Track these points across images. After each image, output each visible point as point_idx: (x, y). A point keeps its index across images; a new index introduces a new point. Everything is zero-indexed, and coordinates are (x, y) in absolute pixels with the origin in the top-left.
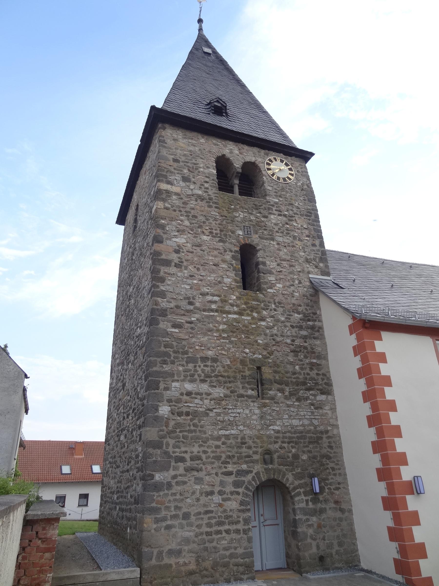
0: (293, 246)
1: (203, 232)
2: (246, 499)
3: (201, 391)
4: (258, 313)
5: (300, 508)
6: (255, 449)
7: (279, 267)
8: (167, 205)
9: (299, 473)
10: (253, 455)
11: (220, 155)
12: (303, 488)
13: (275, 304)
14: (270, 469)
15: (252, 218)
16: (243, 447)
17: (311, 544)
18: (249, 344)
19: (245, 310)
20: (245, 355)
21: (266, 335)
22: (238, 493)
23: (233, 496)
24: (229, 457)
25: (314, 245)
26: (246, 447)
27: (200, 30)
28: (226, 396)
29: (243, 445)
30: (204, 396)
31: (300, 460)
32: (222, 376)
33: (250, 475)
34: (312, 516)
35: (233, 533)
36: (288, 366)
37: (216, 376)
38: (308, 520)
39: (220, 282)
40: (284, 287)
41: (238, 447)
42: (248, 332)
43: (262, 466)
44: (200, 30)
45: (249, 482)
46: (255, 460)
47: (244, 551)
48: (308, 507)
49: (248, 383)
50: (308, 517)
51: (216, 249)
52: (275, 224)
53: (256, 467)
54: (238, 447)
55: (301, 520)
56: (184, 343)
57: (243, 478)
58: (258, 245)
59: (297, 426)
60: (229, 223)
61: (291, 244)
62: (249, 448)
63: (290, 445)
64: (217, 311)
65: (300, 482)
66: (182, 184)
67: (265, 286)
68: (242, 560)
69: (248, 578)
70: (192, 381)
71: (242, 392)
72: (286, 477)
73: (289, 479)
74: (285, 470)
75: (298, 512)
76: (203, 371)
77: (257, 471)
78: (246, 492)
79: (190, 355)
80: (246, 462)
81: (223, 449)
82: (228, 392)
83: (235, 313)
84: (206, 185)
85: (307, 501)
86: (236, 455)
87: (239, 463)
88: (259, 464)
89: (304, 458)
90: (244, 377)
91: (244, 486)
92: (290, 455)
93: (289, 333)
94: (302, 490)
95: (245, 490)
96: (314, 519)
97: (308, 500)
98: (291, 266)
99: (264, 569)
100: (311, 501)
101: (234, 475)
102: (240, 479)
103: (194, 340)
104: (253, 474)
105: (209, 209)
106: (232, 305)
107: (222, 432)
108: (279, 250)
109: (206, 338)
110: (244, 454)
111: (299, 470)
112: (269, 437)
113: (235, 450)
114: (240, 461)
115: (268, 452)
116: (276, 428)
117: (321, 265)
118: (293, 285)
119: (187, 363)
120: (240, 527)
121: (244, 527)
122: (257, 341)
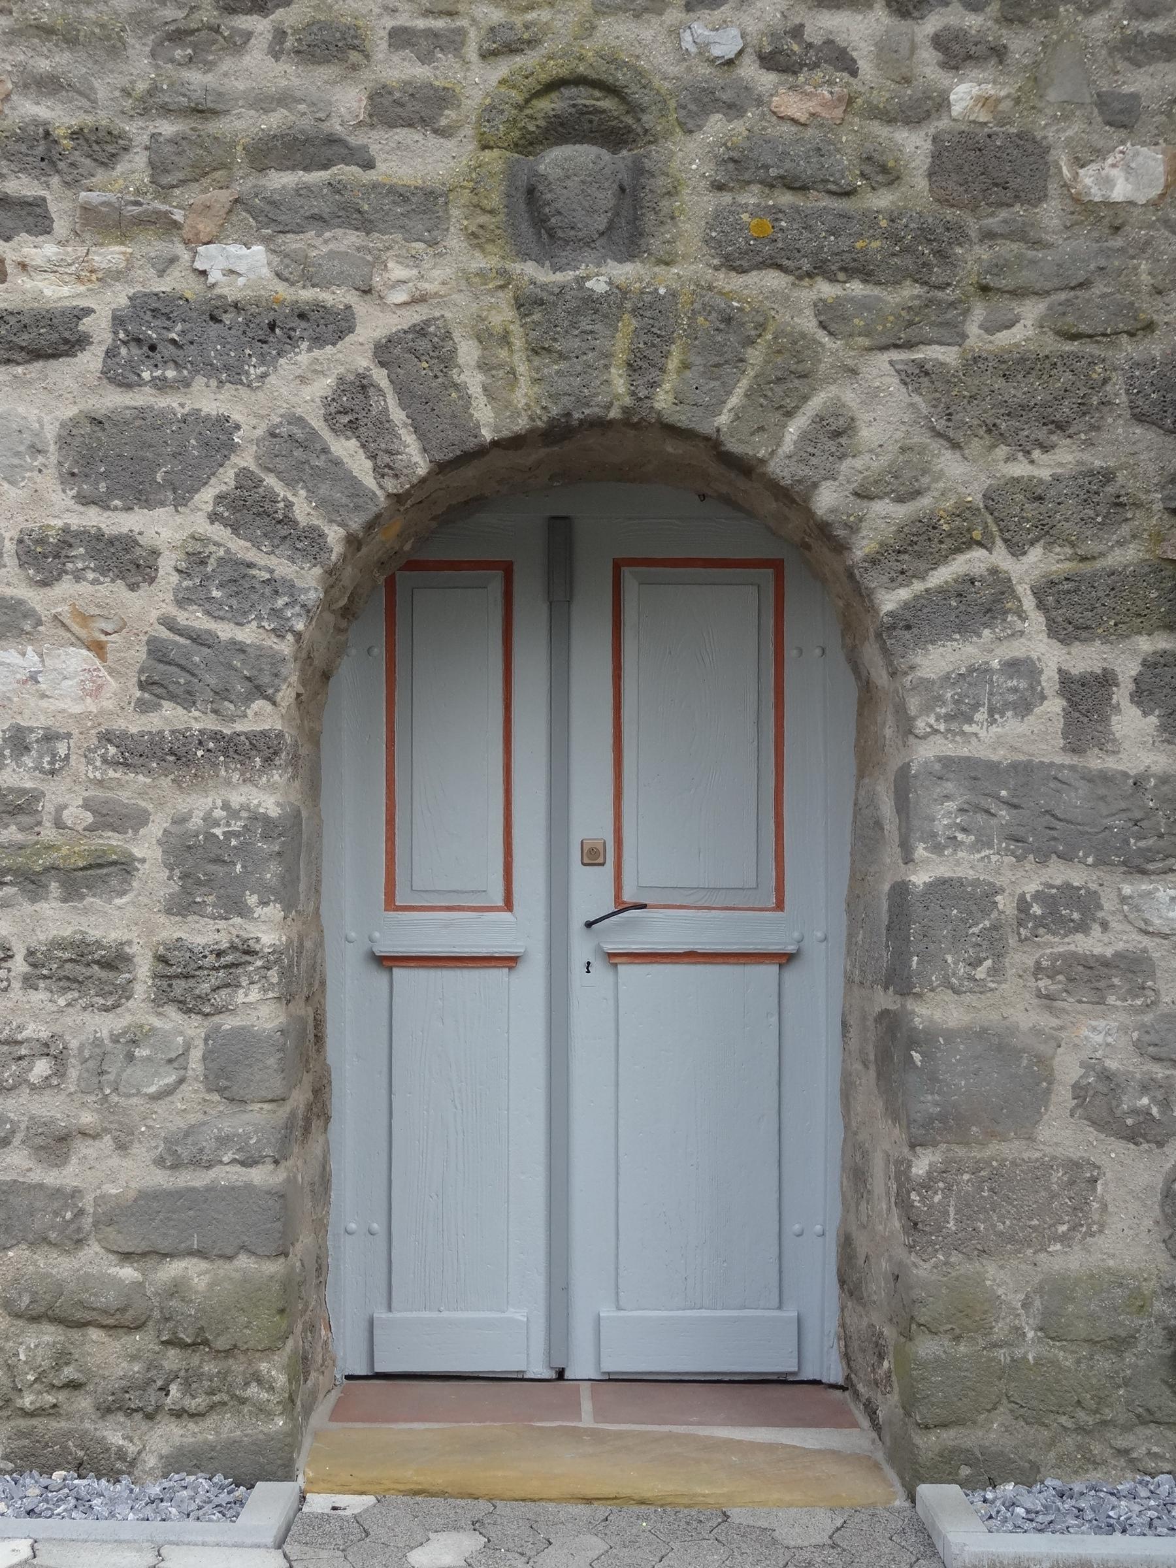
2: (225, 631)
5: (973, 773)
6: (400, 70)
9: (1015, 365)
10: (376, 141)
12: (1045, 532)
14: (591, 302)
16: (239, 43)
17: (1082, 1177)
22: (127, 561)
23: (65, 587)
26: (280, 34)
29: (245, 22)
31: (1050, 214)
33: (304, 356)
34: (1137, 868)
35: (29, 983)
38: (1067, 910)
41: (178, 36)
43: (479, 262)
45: (292, 446)
46: (392, 190)
47: (161, 1179)
48: (1095, 761)
50: (1076, 876)
53: (398, 271)
54: (178, 36)
55: (985, 897)
57: (207, 399)
62: (331, 45)
63: (932, 24)
65: (1020, 469)
68: (128, 1273)
69: (182, 1462)
72: (816, 403)
73: (866, 430)
74: (808, 323)
75: (944, 815)
77: (415, 316)
78: (240, 547)
80: (269, 219)
85: (1087, 697)
86: (138, 131)
87: (168, 226)
88: (455, 242)
89: (1121, 191)
91: (225, 480)
92: (913, 146)
94: (1029, 567)
95: (219, 532)
97: (1106, 680)
99: (581, 1367)
100: (1142, 695)
101: (90, 360)
102: (163, 402)
104: (354, 354)
110: (244, 125)
111: (1026, 328)
113: (139, 67)
114: (193, 195)
115: (593, 110)
120: (126, 920)
121: (171, 930)
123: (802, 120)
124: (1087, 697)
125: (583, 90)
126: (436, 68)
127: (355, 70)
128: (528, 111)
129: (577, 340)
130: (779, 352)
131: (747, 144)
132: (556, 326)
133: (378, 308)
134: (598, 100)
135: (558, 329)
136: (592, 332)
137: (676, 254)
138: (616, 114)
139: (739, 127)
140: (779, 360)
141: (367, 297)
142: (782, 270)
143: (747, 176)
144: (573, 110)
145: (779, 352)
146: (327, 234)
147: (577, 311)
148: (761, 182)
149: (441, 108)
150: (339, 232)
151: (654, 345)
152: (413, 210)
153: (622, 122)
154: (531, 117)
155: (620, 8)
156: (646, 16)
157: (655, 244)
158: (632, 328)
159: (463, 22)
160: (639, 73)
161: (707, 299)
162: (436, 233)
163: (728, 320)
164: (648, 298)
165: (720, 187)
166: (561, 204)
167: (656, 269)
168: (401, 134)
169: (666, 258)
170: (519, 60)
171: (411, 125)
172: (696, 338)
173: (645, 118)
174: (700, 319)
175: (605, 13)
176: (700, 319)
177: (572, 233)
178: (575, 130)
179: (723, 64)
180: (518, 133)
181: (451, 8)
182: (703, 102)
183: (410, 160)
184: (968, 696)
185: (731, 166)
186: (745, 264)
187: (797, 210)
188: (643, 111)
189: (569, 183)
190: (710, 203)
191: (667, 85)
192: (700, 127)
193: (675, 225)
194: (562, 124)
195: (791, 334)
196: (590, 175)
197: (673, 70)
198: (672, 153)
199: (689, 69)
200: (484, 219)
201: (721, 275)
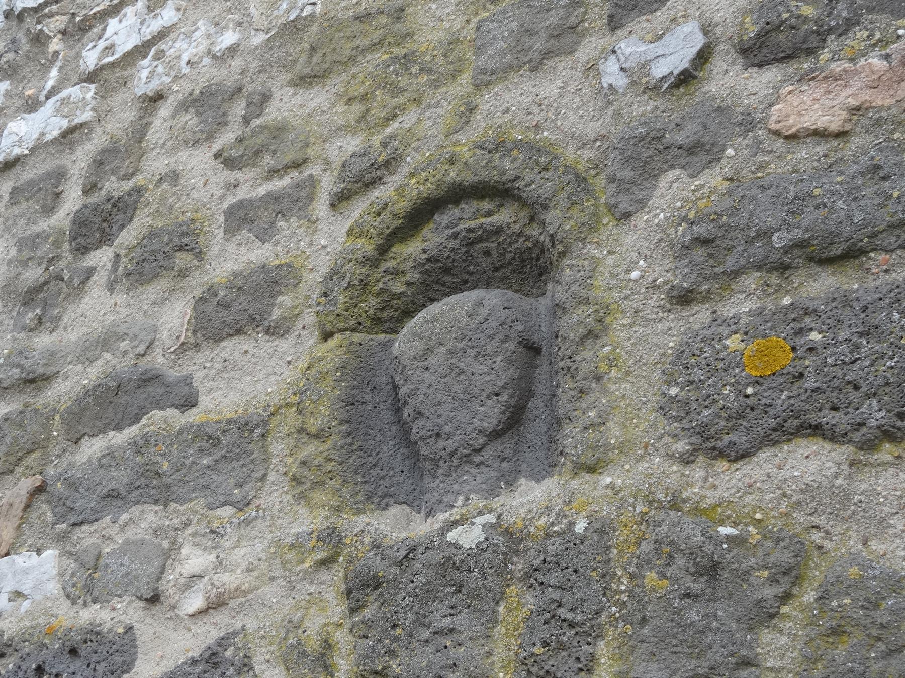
10: (199, 368)
77: (206, 634)
88: (275, 495)
123: (834, 127)
125: (468, 208)
126: (277, 243)
127: (184, 277)
128: (391, 264)
129: (429, 649)
130: (837, 632)
131: (727, 203)
132: (394, 626)
133: (171, 624)
134: (489, 214)
135: (398, 631)
136: (452, 631)
137: (607, 447)
138: (517, 228)
139: (714, 178)
140: (840, 652)
141: (155, 609)
142: (824, 437)
143: (730, 263)
144: (454, 243)
145: (837, 632)
146: (124, 517)
147: (428, 594)
148: (759, 267)
149: (274, 296)
150: (136, 510)
151: (562, 647)
152: (224, 457)
153: (528, 238)
154: (396, 273)
155: (511, 67)
156: (549, 63)
157: (572, 437)
158: (524, 613)
159: (314, 170)
160: (533, 149)
161: (664, 528)
162: (247, 487)
163: (711, 570)
164: (554, 546)
165: (684, 298)
166: (421, 398)
167: (575, 483)
168: (231, 348)
169: (588, 458)
170: (379, 194)
171: (239, 332)
172: (644, 621)
173: (548, 217)
174: (651, 577)
175: (488, 84)
176: (651, 577)
177: (441, 444)
178: (471, 274)
179: (676, 85)
180: (373, 302)
181: (299, 156)
182: (647, 155)
183: (248, 378)
185: (699, 254)
186: (740, 438)
187: (846, 301)
188: (545, 207)
189: (432, 360)
190: (669, 332)
191: (587, 153)
192: (642, 203)
193: (605, 392)
194: (446, 271)
195: (858, 584)
196: (463, 337)
197: (593, 128)
198: (596, 262)
199: (618, 115)
200: (310, 449)
201: (697, 472)
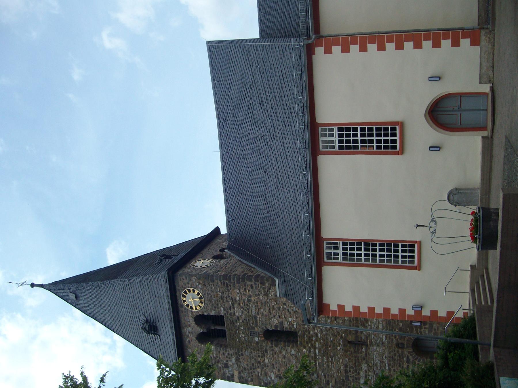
0: (257, 302)
1: (263, 362)
3: (364, 375)
4: (312, 337)
7: (276, 317)
8: (250, 379)
11: (197, 341)
13: (304, 325)
15: (242, 328)
18: (334, 346)
19: (312, 345)
20: (341, 350)
21: (327, 334)
24: (400, 366)
25: (252, 286)
27: (42, 286)
28: (366, 363)
30: (367, 374)
32: (355, 364)
36: (346, 324)
37: (355, 366)
39: (296, 356)
40: (291, 317)
42: (326, 345)
44: (42, 286)
45: (413, 357)
49: (358, 350)
51: (273, 356)
52: (242, 312)
56: (337, 380)
58: (263, 328)
59: (383, 326)
60: (251, 345)
61: (256, 304)
64: (315, 361)
66: (230, 369)
67: (293, 329)
70: (359, 379)
71: (363, 354)
76: (353, 373)
79: (344, 378)
80: (403, 358)
81: (396, 368)
82: (364, 362)
83: (315, 351)
84: (226, 354)
85: (425, 328)
90: (355, 352)
93: (324, 319)
94: (419, 330)
96: (434, 325)
98: (273, 308)
103: (335, 376)
104: (409, 355)
105: (244, 355)
106: (310, 352)
107: (387, 368)
108: (262, 314)
109: (333, 369)
112: (389, 343)
115: (398, 345)
116: (384, 338)
117: (267, 284)
118: (288, 310)
119: (349, 380)
122: (332, 341)
124: (425, 328)
183: (400, 352)
184: (425, 333)
